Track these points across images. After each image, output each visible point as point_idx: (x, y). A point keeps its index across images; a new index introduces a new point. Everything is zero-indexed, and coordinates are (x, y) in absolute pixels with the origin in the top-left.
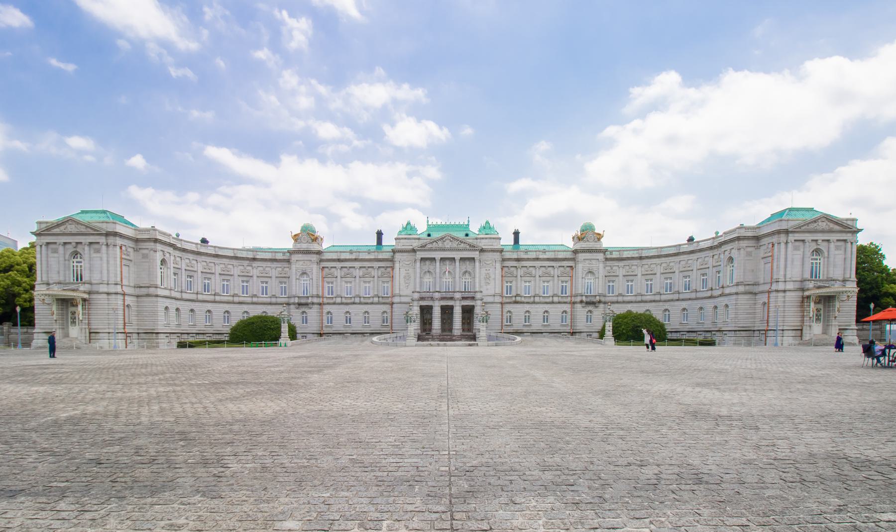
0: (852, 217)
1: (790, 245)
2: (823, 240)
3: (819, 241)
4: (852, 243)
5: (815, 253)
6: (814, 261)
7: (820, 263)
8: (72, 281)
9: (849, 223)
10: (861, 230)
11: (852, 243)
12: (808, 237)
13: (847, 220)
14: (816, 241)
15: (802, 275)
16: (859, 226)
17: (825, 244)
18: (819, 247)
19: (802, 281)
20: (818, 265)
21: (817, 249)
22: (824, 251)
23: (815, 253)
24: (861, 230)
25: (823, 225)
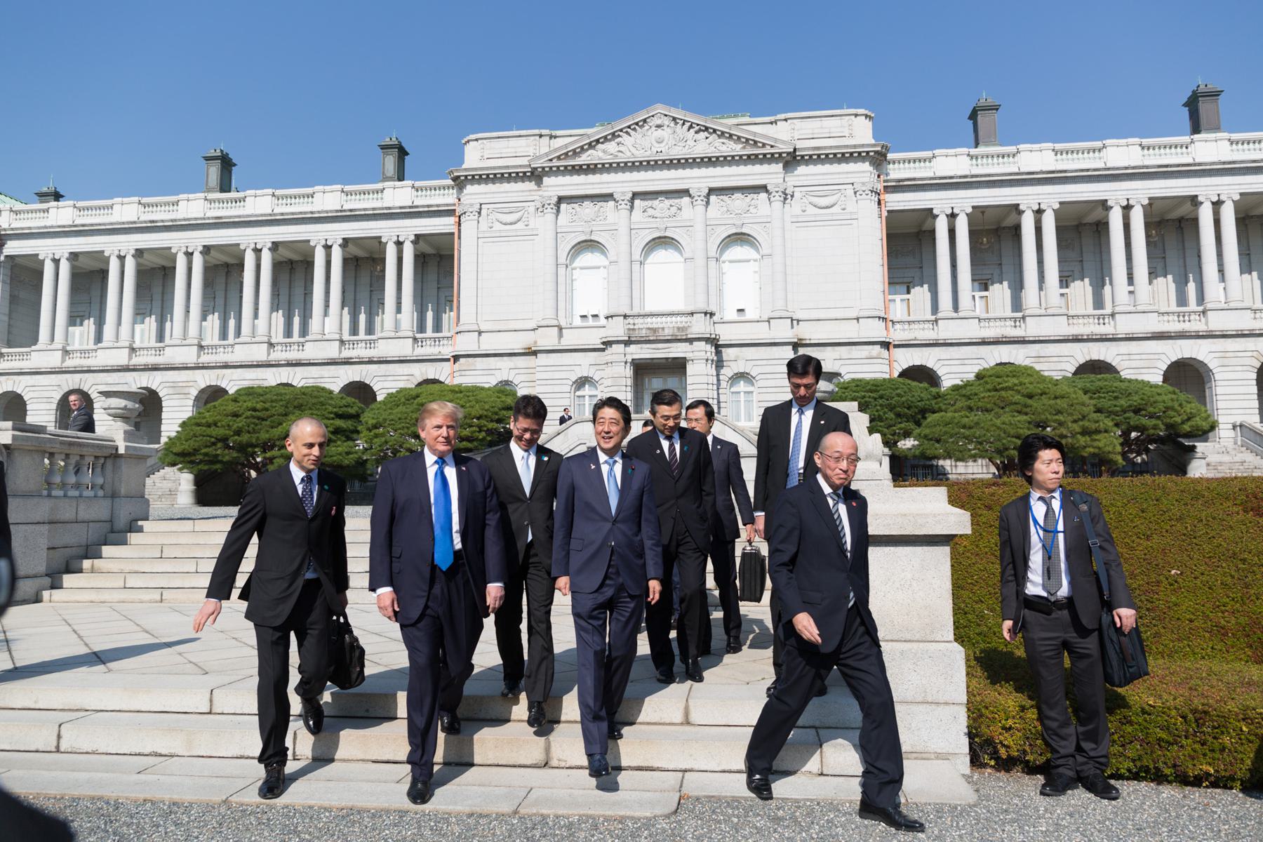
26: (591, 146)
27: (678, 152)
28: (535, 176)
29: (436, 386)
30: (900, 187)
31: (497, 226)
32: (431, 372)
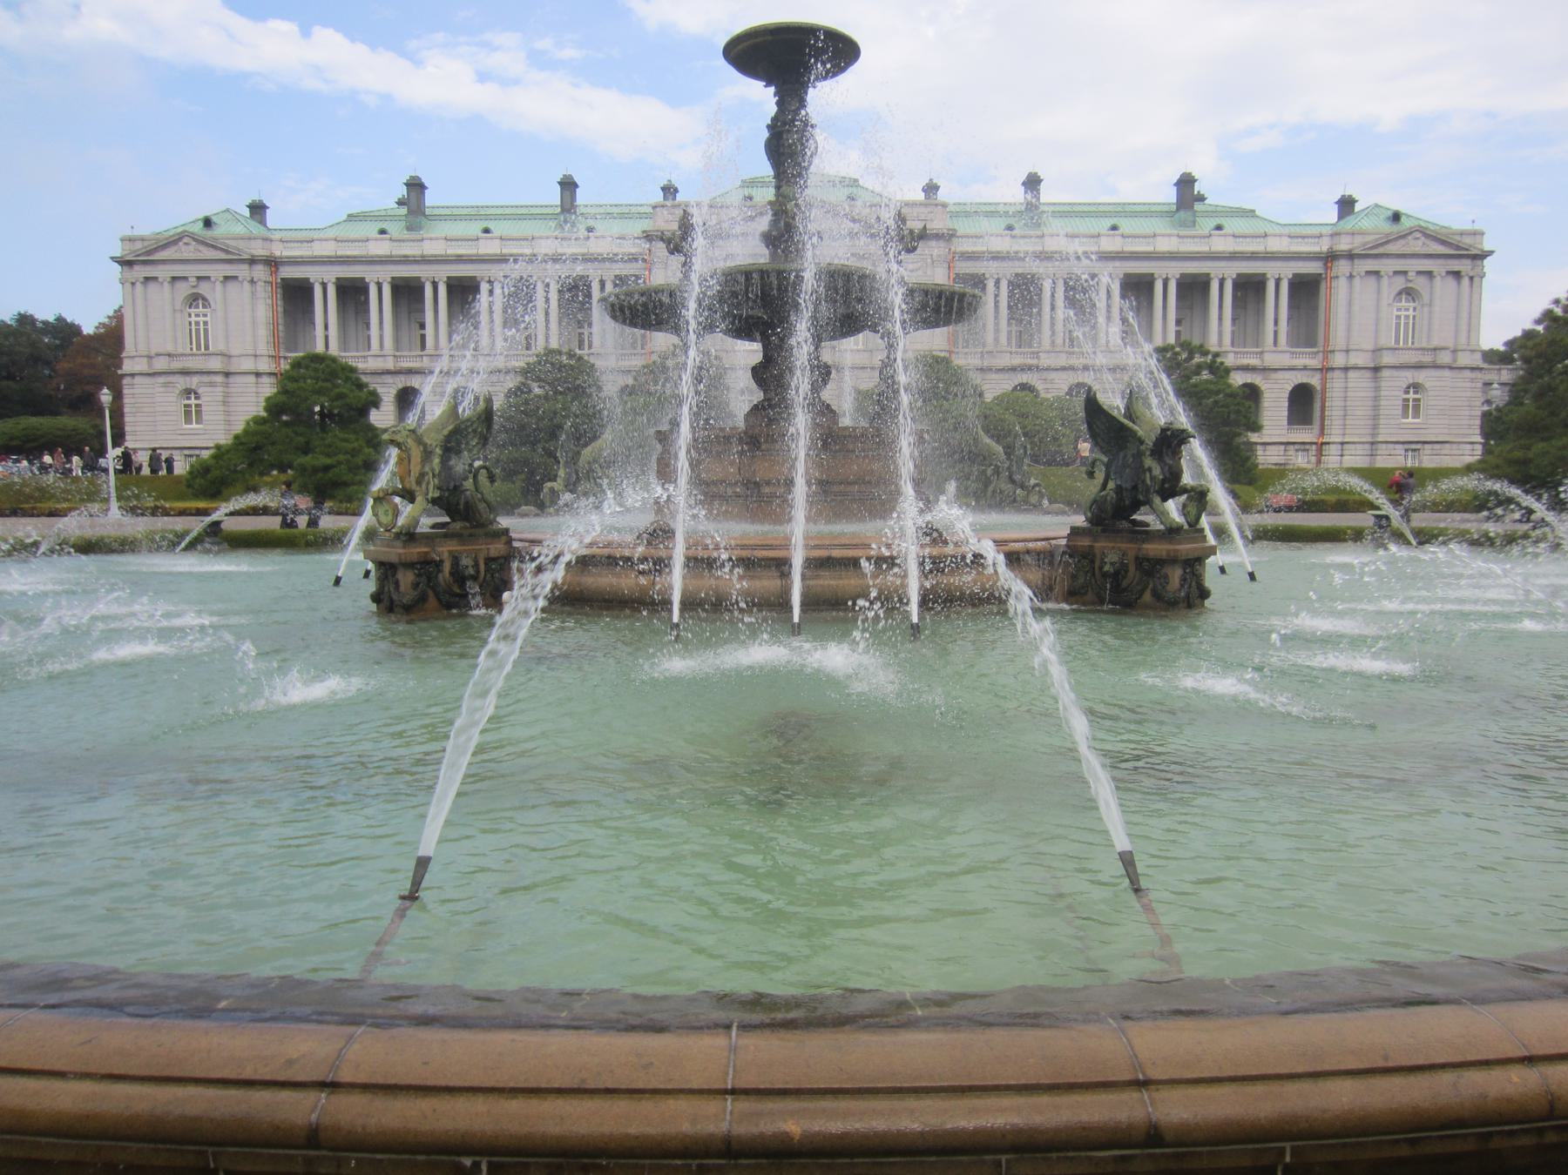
0: (1477, 227)
1: (1357, 281)
2: (1419, 273)
3: (1410, 274)
4: (1471, 278)
5: (1404, 296)
6: (1403, 313)
7: (1414, 317)
8: (188, 351)
9: (1467, 240)
10: (1490, 253)
11: (1471, 278)
12: (1387, 266)
13: (1462, 234)
14: (1405, 273)
15: (1376, 337)
16: (1487, 247)
17: (1422, 280)
18: (1410, 285)
19: (1377, 351)
20: (1411, 322)
21: (1406, 288)
22: (1423, 294)
23: (1404, 296)
24: (1492, 252)
25: (1417, 245)
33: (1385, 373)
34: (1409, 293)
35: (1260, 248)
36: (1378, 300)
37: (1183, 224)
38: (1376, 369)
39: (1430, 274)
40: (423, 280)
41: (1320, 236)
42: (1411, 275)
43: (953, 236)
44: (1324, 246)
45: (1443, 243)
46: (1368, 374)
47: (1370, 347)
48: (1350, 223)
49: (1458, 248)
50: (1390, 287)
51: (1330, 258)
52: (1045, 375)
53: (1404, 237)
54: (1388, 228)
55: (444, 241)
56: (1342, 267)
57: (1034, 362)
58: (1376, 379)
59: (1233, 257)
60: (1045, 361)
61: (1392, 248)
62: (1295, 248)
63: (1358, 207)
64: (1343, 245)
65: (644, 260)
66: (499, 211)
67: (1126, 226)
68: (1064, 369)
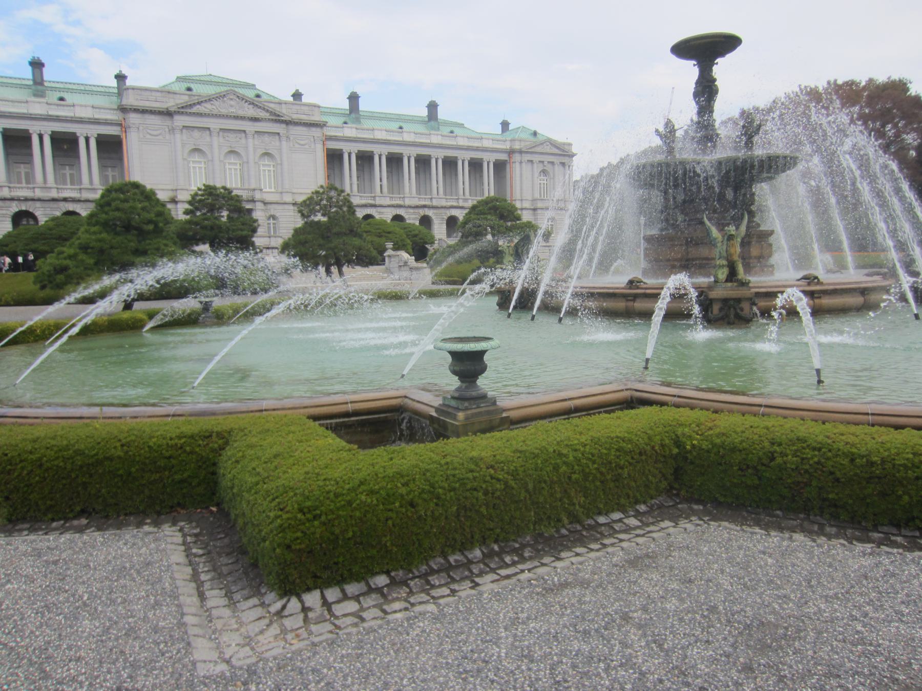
0: (569, 141)
1: (524, 164)
9: (566, 147)
12: (536, 158)
14: (543, 162)
25: (548, 149)
26: (199, 103)
27: (241, 113)
28: (168, 114)
29: (74, 217)
30: (330, 138)
31: (148, 136)
32: (71, 207)
33: (539, 212)
34: (544, 172)
35: (480, 145)
36: (533, 175)
37: (433, 128)
38: (535, 210)
39: (552, 163)
40: (78, 135)
41: (505, 141)
42: (546, 163)
43: (325, 125)
44: (507, 146)
45: (558, 148)
46: (531, 212)
47: (530, 198)
48: (508, 136)
49: (564, 151)
50: (538, 168)
51: (511, 152)
52: (379, 209)
53: (542, 144)
54: (532, 138)
55: (90, 109)
56: (517, 157)
57: (372, 202)
58: (534, 215)
59: (468, 149)
60: (378, 201)
61: (538, 149)
62: (471, 144)
63: (511, 127)
64: (517, 146)
65: (121, 125)
66: (62, 86)
67: (406, 127)
68: (389, 206)
